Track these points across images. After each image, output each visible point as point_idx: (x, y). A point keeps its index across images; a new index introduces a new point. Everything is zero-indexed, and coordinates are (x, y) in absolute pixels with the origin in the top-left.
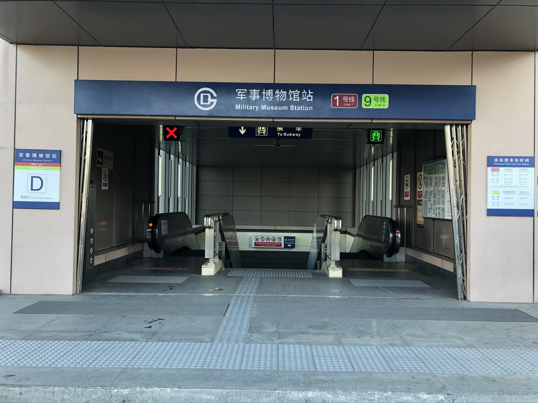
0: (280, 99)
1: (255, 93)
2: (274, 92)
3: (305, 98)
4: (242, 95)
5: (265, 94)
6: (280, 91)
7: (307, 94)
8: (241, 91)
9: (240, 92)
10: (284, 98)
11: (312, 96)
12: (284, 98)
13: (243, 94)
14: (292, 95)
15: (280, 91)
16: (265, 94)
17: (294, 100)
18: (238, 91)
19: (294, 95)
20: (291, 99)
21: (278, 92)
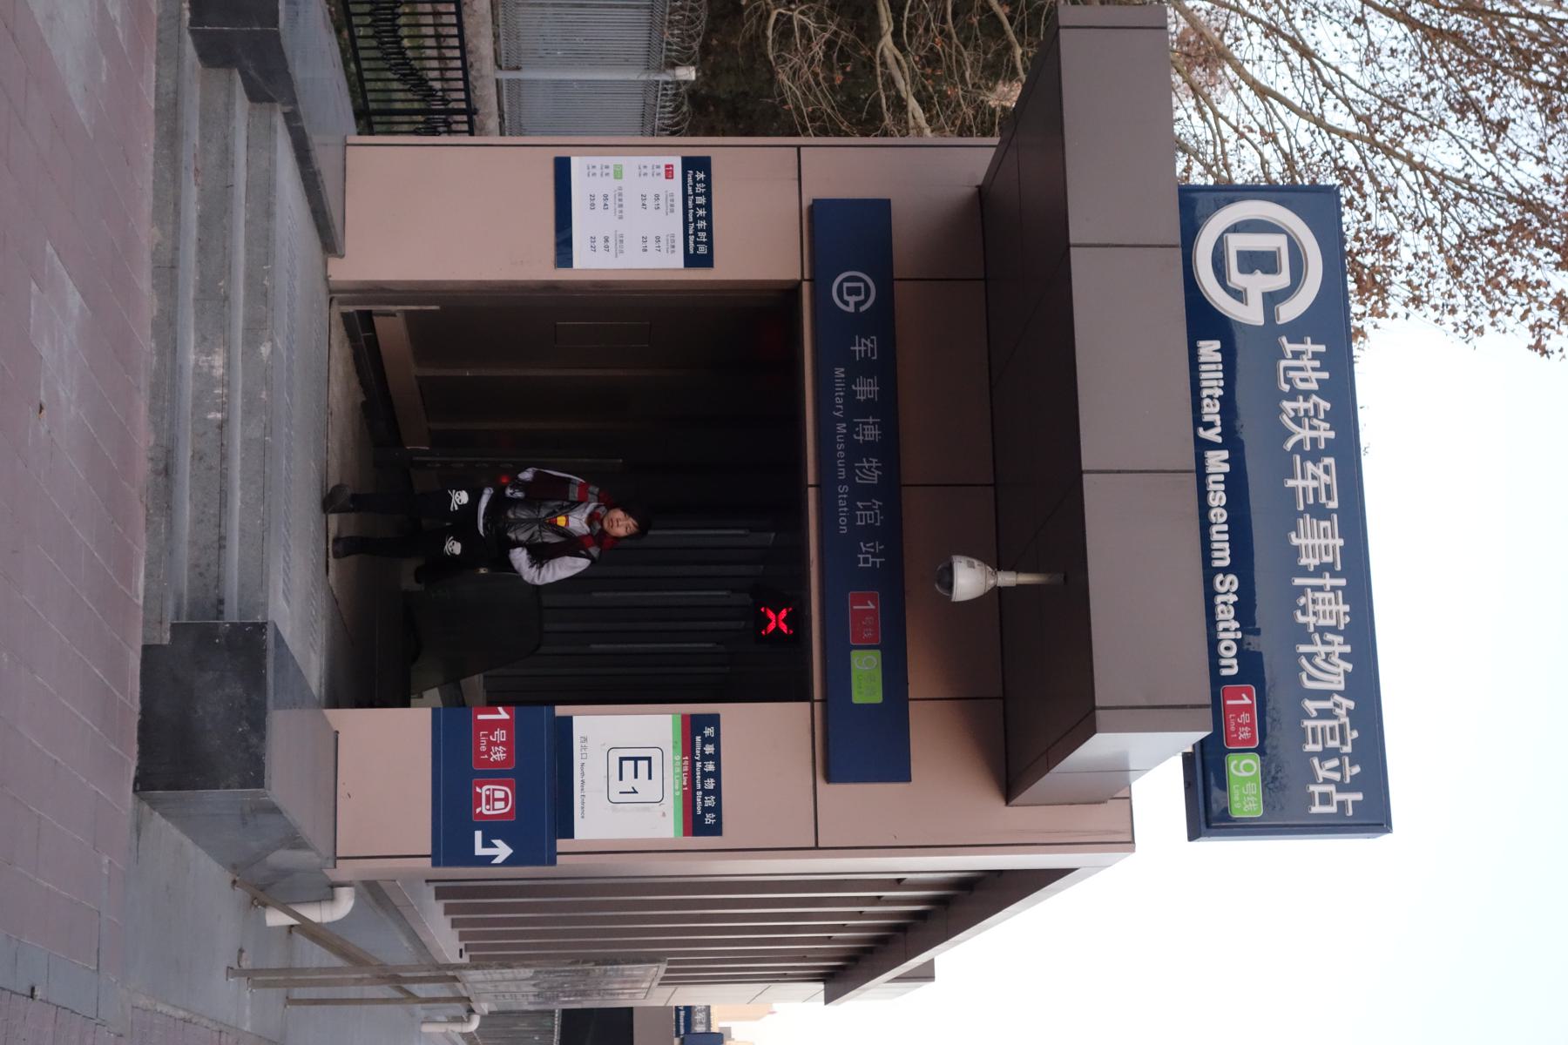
0: (1310, 657)
1: (1323, 542)
2: (1334, 630)
3: (1321, 774)
4: (1311, 484)
5: (1321, 589)
6: (1343, 656)
7: (1341, 787)
8: (1328, 487)
9: (1324, 478)
10: (1310, 678)
11: (1333, 809)
12: (1310, 678)
13: (1316, 490)
14: (1325, 714)
15: (1343, 656)
16: (1321, 589)
17: (1308, 724)
18: (1327, 470)
19: (1328, 723)
20: (1311, 706)
21: (1338, 649)
